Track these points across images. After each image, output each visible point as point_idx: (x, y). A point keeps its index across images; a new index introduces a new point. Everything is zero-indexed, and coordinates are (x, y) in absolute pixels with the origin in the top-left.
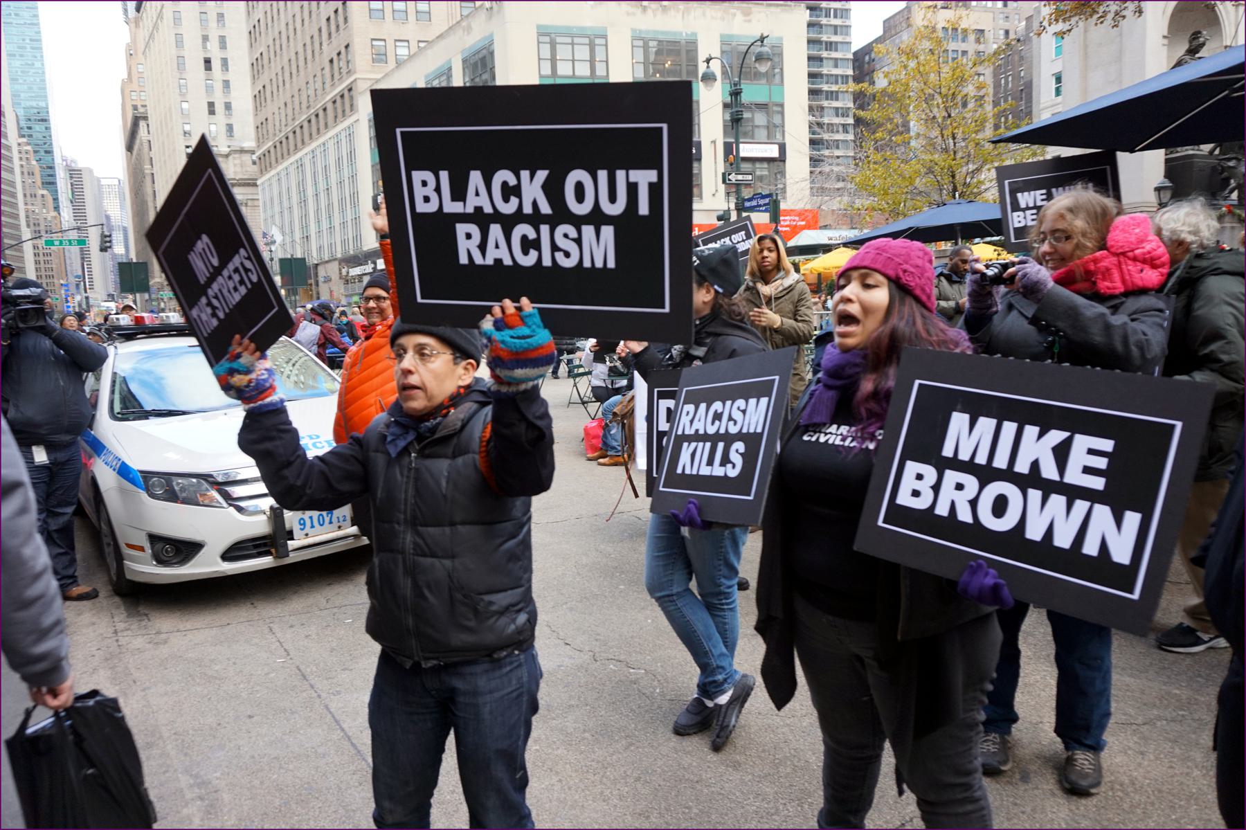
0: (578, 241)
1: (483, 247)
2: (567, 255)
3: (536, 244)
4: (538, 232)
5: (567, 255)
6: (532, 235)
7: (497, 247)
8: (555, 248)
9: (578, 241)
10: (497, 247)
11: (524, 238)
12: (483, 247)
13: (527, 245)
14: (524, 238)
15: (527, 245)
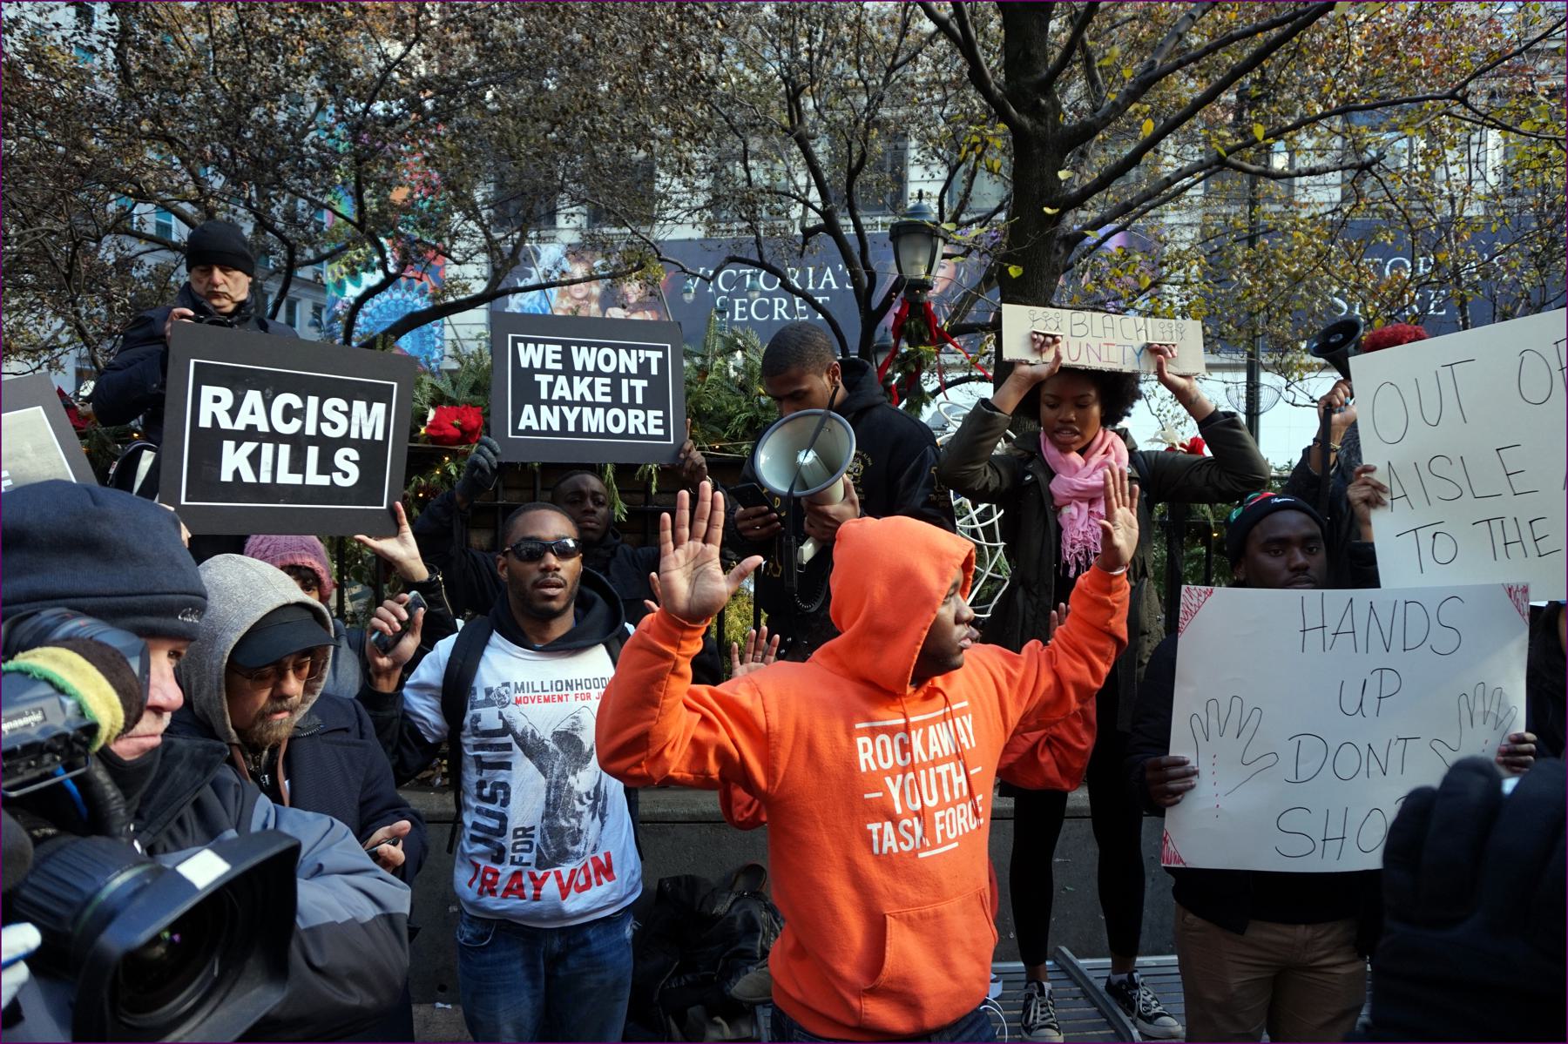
0: (348, 414)
1: (233, 413)
2: (334, 426)
3: (301, 414)
4: (305, 402)
5: (334, 426)
6: (296, 402)
7: (253, 413)
8: (321, 418)
9: (348, 414)
10: (253, 413)
11: (288, 407)
12: (233, 413)
13: (289, 414)
14: (288, 407)
15: (289, 414)
